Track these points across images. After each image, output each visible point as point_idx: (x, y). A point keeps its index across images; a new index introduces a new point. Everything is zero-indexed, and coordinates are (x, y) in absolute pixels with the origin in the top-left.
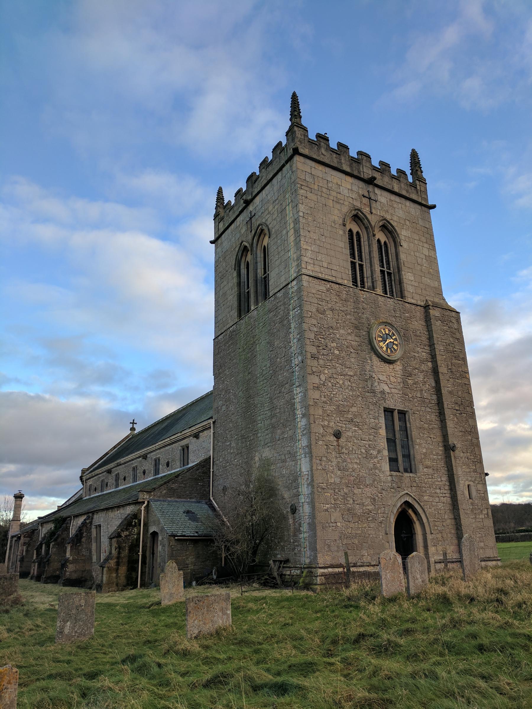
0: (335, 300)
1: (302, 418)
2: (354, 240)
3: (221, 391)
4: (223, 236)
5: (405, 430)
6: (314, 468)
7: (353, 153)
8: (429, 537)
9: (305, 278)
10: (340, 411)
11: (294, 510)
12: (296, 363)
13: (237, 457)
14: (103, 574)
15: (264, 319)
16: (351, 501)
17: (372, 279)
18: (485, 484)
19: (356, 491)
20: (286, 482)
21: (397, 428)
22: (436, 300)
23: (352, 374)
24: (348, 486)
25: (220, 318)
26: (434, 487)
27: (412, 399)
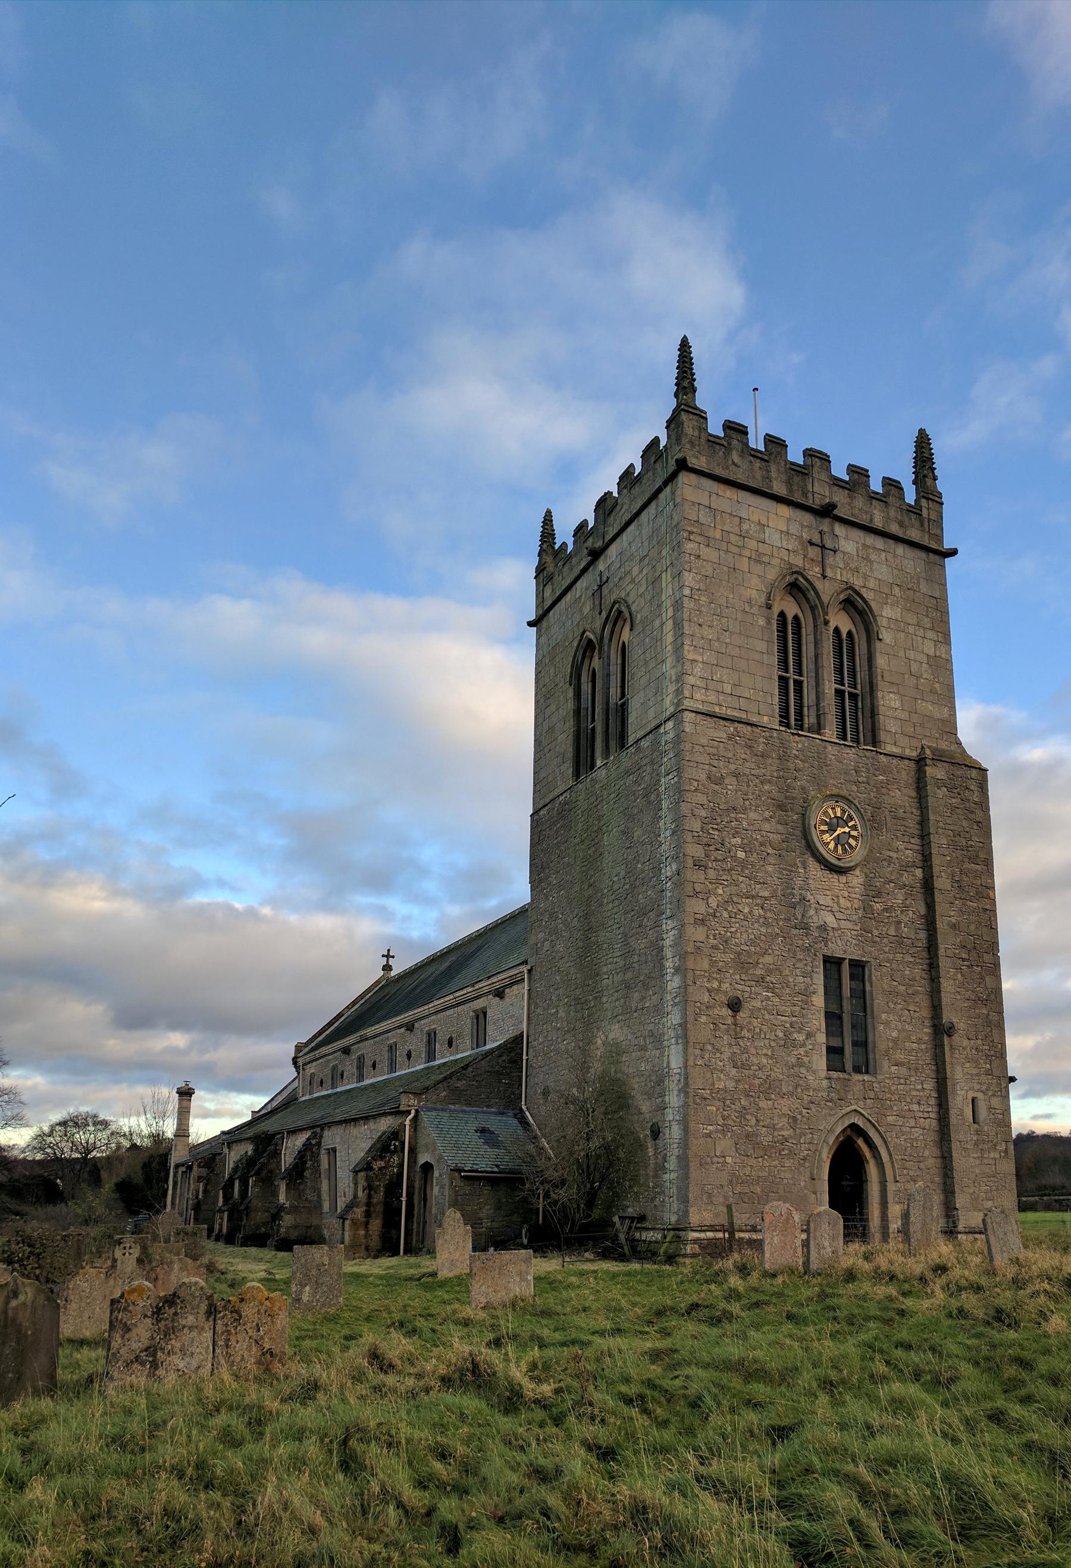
0: (743, 756)
1: (674, 974)
2: (787, 632)
3: (542, 914)
4: (551, 613)
5: (861, 996)
6: (690, 1063)
7: (795, 455)
8: (891, 1187)
9: (688, 716)
10: (742, 964)
11: (656, 1133)
12: (669, 874)
13: (567, 1036)
14: (343, 1230)
15: (617, 787)
16: (753, 1122)
17: (818, 710)
18: (1006, 1097)
19: (763, 1104)
20: (646, 1085)
21: (846, 992)
22: (943, 745)
23: (766, 894)
24: (748, 1095)
25: (542, 776)
26: (908, 1100)
27: (878, 939)
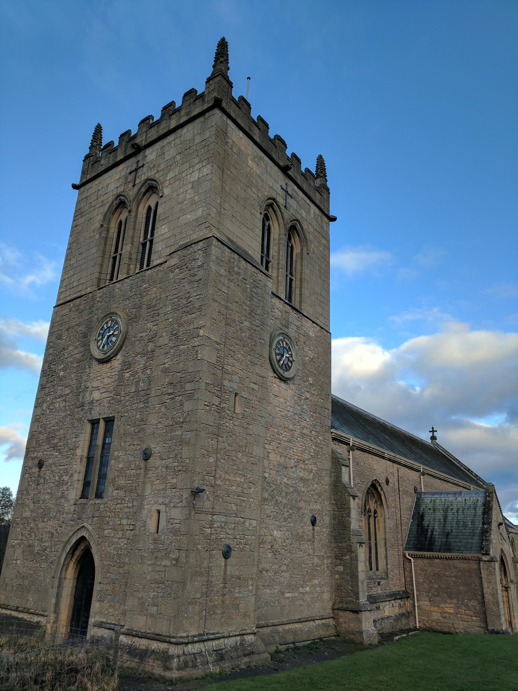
26: (121, 516)
